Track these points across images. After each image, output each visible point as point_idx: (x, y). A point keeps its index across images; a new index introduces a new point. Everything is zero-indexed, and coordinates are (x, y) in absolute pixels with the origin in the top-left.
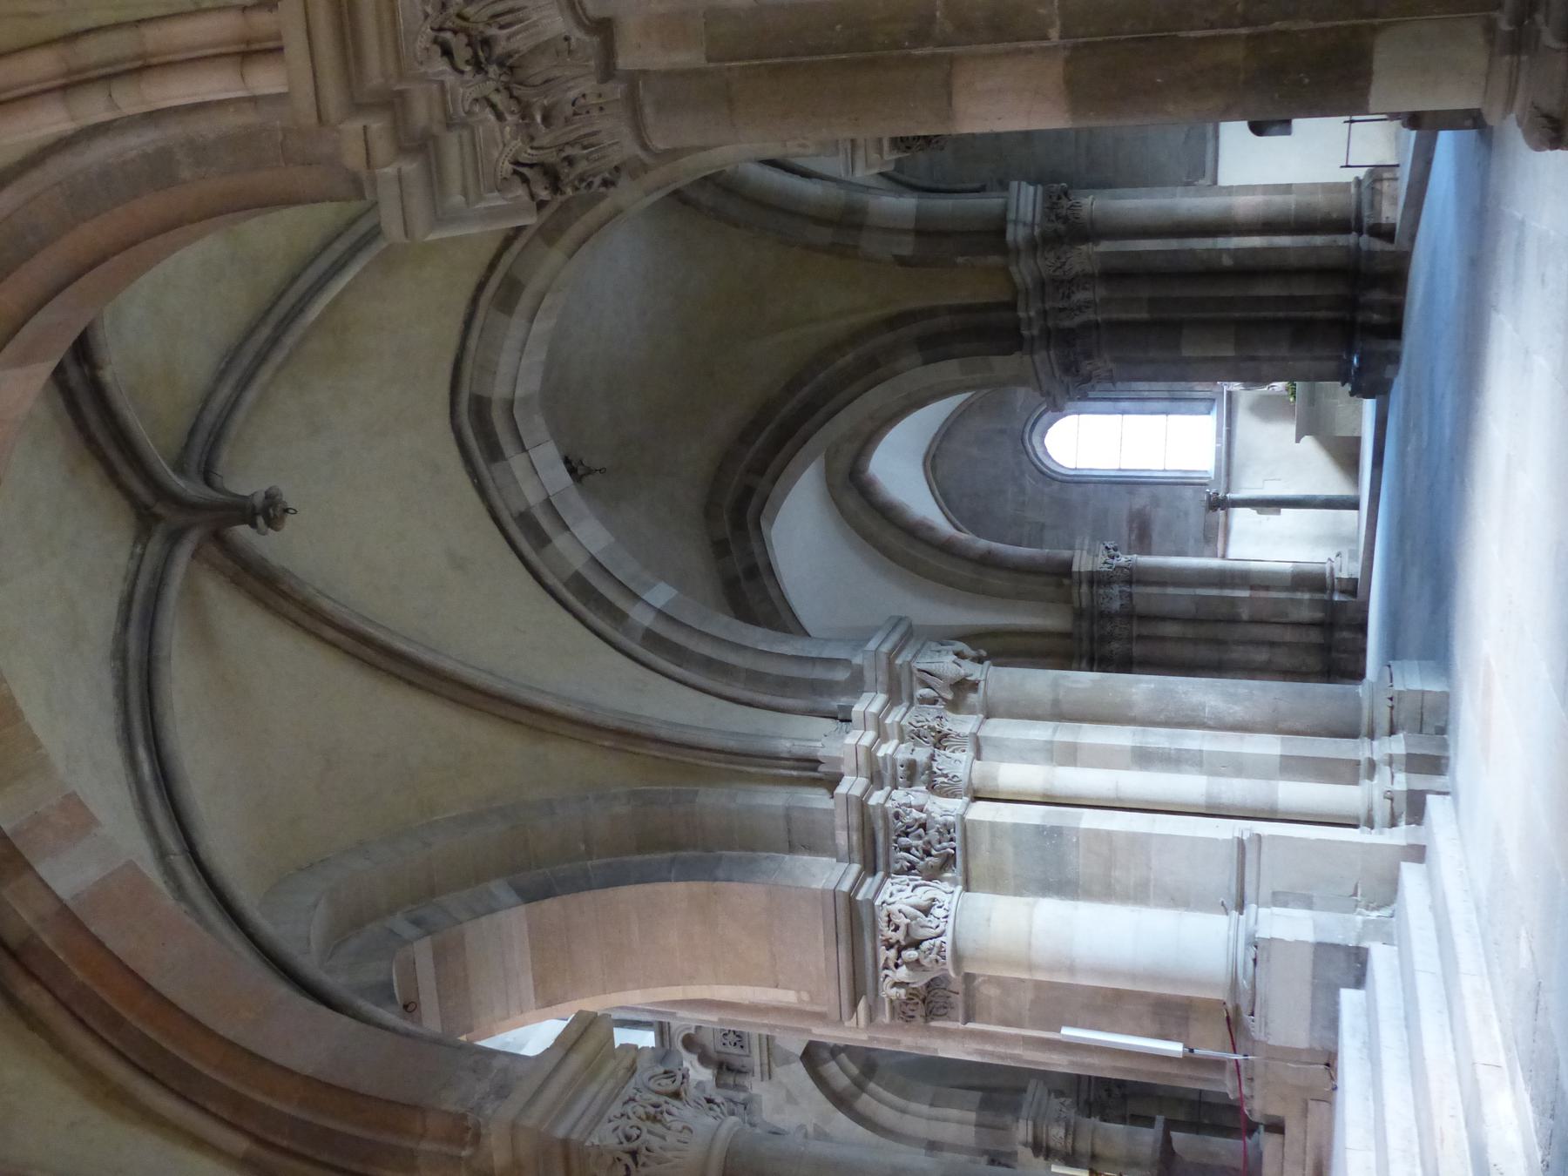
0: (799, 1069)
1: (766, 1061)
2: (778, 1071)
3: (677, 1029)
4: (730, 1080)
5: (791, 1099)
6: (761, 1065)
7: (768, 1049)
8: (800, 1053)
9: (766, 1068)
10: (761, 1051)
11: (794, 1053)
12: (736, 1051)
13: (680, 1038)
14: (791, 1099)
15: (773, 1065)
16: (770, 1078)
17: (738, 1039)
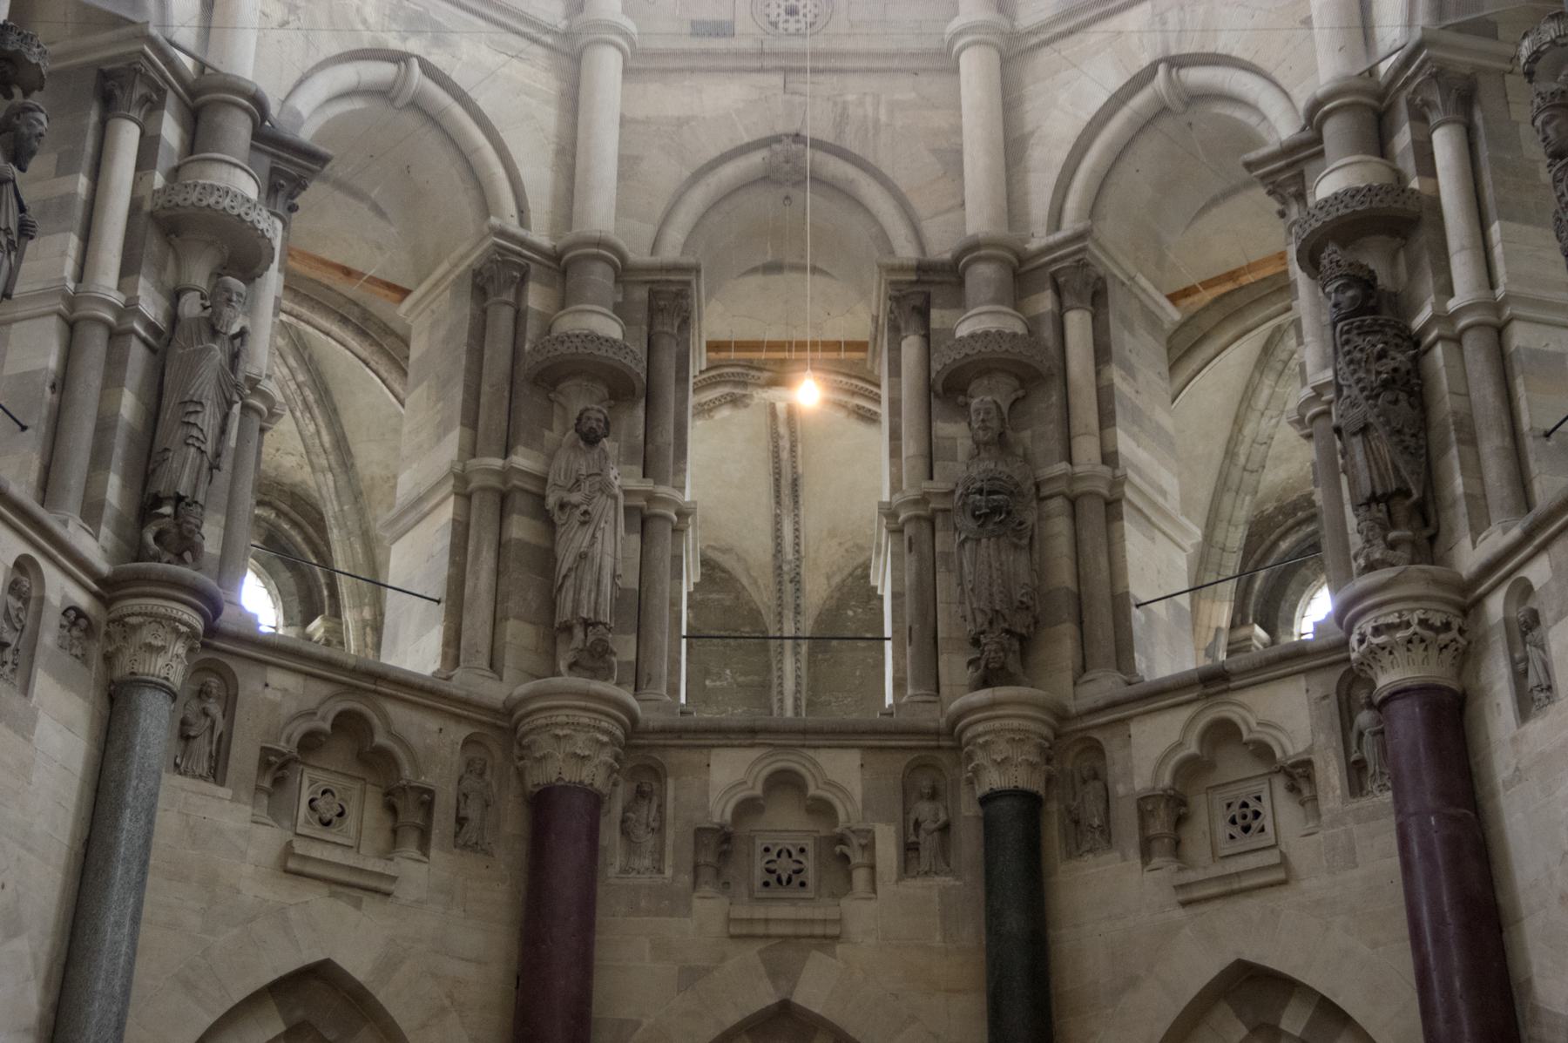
0: (764, 996)
1: (775, 929)
2: (751, 953)
3: (815, 764)
4: (709, 857)
5: (690, 977)
6: (767, 921)
7: (797, 937)
8: (799, 999)
9: (760, 929)
10: (796, 921)
11: (794, 986)
12: (759, 874)
13: (797, 767)
14: (690, 977)
15: (761, 945)
16: (732, 937)
17: (784, 878)
